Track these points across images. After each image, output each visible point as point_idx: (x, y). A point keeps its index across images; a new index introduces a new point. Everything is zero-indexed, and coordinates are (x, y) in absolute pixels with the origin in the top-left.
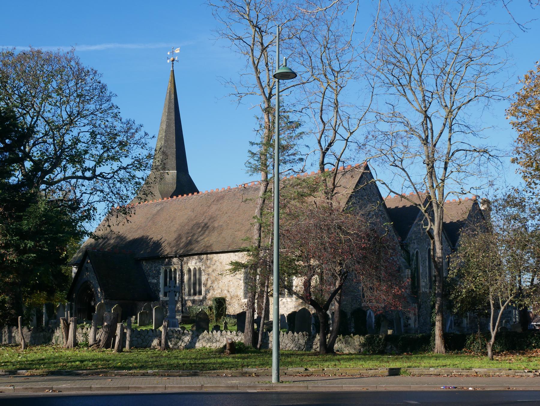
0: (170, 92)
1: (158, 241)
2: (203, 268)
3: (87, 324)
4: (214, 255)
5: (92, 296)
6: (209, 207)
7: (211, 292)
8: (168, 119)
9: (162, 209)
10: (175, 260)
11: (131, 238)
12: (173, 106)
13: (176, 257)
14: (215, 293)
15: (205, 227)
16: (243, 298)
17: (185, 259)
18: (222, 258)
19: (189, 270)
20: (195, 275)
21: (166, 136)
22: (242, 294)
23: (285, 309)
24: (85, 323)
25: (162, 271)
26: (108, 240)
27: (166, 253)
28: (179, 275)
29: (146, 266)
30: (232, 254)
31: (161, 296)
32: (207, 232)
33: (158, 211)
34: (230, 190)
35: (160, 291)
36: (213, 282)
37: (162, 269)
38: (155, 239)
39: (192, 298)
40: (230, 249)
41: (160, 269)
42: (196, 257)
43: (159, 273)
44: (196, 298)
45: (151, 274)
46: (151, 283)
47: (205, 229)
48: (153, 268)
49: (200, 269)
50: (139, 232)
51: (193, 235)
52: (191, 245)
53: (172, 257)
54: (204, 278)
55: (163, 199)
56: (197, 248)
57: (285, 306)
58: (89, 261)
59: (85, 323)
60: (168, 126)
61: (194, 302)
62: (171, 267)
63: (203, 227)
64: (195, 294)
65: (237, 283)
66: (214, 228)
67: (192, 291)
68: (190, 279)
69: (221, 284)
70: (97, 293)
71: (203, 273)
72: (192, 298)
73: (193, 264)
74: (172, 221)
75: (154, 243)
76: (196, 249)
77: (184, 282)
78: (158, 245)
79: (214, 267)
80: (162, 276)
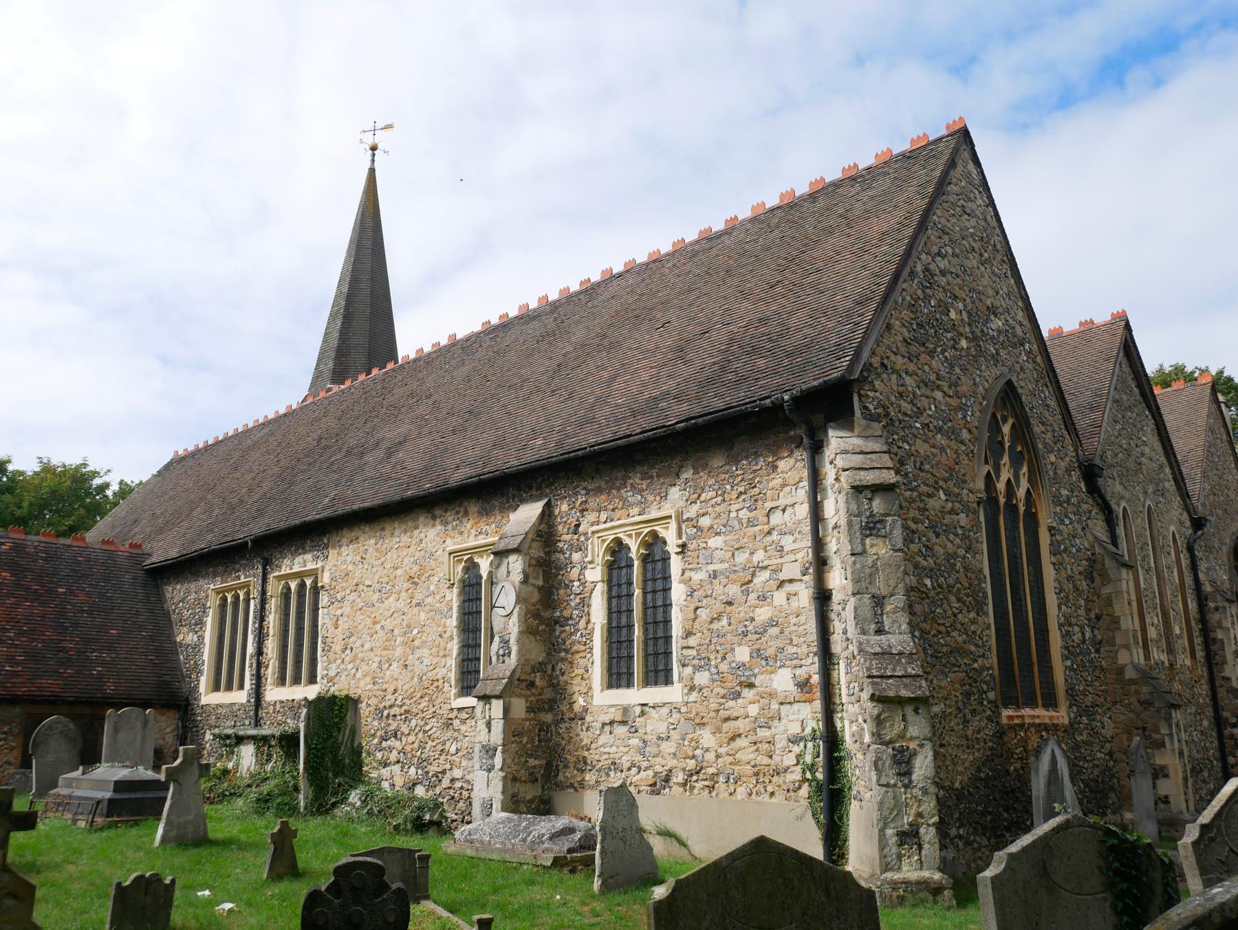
22: (453, 676)
23: (635, 742)
31: (204, 683)
80: (209, 621)
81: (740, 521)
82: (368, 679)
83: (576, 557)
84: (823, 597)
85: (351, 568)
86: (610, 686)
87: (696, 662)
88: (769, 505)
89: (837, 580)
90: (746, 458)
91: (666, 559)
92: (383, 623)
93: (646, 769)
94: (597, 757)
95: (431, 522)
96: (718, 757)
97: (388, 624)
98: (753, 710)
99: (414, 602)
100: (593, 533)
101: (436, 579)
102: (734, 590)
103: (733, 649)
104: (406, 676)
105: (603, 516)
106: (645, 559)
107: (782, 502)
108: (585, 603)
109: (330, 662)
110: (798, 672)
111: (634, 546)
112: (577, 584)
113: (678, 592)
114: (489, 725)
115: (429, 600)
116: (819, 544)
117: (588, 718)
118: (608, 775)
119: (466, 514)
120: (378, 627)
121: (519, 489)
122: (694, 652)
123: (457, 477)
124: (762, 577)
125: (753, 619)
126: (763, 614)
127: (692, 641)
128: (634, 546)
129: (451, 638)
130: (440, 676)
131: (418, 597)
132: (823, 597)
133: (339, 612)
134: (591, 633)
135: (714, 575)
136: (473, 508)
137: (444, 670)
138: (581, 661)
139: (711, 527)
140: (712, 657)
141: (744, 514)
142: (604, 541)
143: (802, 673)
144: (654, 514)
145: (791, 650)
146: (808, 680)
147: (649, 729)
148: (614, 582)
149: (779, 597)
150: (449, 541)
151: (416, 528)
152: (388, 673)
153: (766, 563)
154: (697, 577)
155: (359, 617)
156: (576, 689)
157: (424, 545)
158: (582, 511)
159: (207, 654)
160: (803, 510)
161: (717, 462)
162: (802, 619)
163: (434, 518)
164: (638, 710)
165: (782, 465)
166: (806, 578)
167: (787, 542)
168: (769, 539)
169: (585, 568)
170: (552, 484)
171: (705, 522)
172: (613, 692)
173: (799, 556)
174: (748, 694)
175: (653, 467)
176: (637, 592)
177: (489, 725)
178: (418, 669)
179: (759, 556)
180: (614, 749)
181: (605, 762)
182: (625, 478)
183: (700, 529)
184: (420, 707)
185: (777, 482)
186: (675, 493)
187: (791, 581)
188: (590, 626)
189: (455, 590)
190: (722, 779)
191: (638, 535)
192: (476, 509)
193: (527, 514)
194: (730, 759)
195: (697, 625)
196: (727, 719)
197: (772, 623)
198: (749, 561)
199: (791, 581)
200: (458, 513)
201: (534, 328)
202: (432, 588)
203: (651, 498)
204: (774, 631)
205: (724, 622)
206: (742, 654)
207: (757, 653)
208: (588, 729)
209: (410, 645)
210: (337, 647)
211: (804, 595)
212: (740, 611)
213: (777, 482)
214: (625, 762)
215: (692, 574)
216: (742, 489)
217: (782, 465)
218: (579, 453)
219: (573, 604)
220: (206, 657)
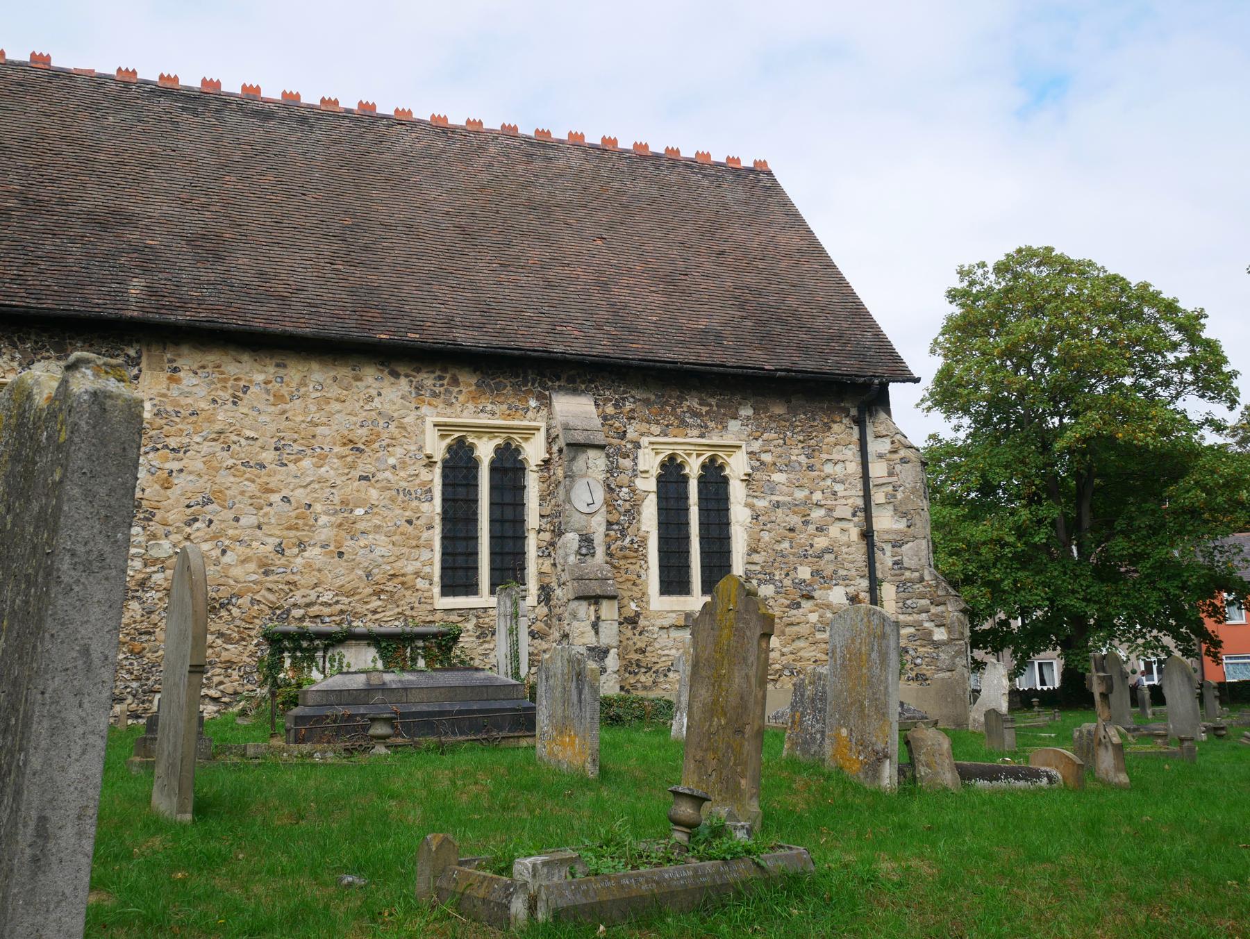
16: (437, 590)
65: (397, 515)
82: (252, 566)
83: (626, 463)
84: (867, 535)
85: (203, 405)
86: (664, 591)
87: (760, 576)
88: (825, 456)
89: (885, 522)
90: (805, 414)
92: (284, 493)
94: (654, 660)
95: (392, 379)
96: (783, 655)
97: (300, 495)
98: (813, 618)
99: (356, 473)
100: (650, 443)
101: (399, 451)
102: (795, 520)
103: (795, 568)
104: (341, 567)
105: (656, 429)
106: (702, 480)
107: (835, 457)
109: (154, 536)
110: (848, 590)
111: (693, 469)
112: (625, 490)
113: (739, 514)
114: (595, 626)
115: (388, 474)
116: (867, 496)
117: (642, 622)
118: (666, 676)
119: (455, 382)
120: (275, 498)
121: (542, 375)
122: (758, 568)
123: (466, 338)
124: (817, 514)
125: (812, 546)
126: (821, 542)
127: (756, 558)
128: (693, 469)
129: (430, 527)
130: (410, 568)
131: (365, 466)
132: (867, 535)
133: (175, 466)
134: (644, 541)
135: (778, 505)
136: (468, 381)
137: (418, 564)
138: (632, 567)
139: (775, 464)
140: (777, 573)
141: (803, 459)
142: (657, 453)
143: (851, 590)
144: (715, 440)
145: (842, 572)
146: (857, 596)
149: (834, 530)
151: (358, 379)
152: (299, 560)
153: (822, 503)
154: (761, 504)
155: (225, 479)
157: (377, 402)
158: (630, 418)
160: (854, 467)
161: (779, 410)
162: (853, 549)
163: (396, 375)
165: (835, 427)
166: (856, 519)
167: (839, 488)
169: (636, 476)
170: (591, 381)
171: (767, 458)
172: (666, 598)
173: (850, 501)
174: (807, 605)
175: (712, 396)
177: (595, 626)
178: (364, 558)
179: (817, 496)
181: (662, 665)
182: (681, 399)
183: (762, 463)
184: (372, 606)
185: (831, 440)
186: (734, 425)
187: (840, 520)
188: (641, 533)
189: (438, 470)
190: (787, 672)
192: (474, 381)
193: (575, 409)
194: (793, 657)
195: (762, 545)
196: (792, 624)
197: (829, 550)
198: (808, 498)
199: (840, 520)
200: (441, 378)
201: (254, 131)
202: (392, 461)
203: (712, 425)
204: (832, 556)
205: (786, 545)
206: (804, 573)
207: (816, 573)
208: (641, 634)
209: (348, 527)
210: (176, 516)
211: (854, 533)
212: (802, 538)
213: (831, 440)
215: (755, 501)
216: (801, 438)
217: (835, 427)
218: (668, 365)
219: (622, 510)
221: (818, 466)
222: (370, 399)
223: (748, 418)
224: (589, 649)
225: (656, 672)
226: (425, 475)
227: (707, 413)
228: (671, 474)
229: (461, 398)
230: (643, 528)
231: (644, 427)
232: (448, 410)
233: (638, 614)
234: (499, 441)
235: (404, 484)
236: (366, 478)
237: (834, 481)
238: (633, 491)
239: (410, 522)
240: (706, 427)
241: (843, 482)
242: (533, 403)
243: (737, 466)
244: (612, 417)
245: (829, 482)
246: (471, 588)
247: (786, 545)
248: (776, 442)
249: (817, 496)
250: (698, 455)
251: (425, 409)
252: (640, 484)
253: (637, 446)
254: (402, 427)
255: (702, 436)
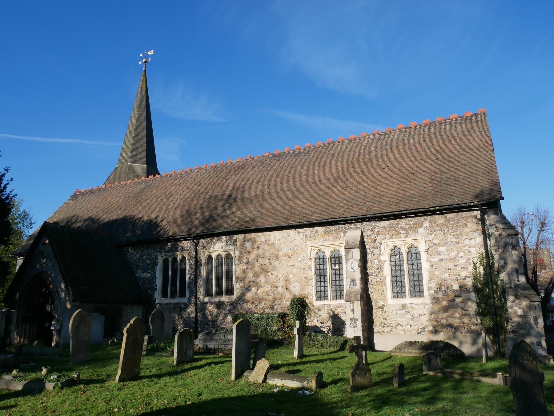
0: (141, 89)
1: (151, 221)
2: (235, 254)
3: (49, 373)
4: (260, 234)
5: (51, 296)
6: (225, 178)
7: (254, 289)
8: (138, 114)
9: (148, 187)
10: (186, 244)
11: (107, 220)
12: (144, 103)
13: (185, 239)
14: (259, 292)
15: (230, 200)
16: (314, 298)
17: (203, 242)
18: (272, 238)
19: (210, 258)
20: (220, 265)
21: (136, 130)
22: (314, 293)
23: (408, 316)
24: (44, 371)
25: (160, 260)
26: (73, 223)
27: (170, 234)
28: (190, 266)
29: (133, 254)
30: (292, 232)
31: (158, 296)
32: (236, 206)
33: (143, 189)
34: (251, 159)
35: (156, 290)
36: (257, 275)
37: (159, 257)
38: (145, 218)
39: (217, 299)
40: (290, 223)
41: (157, 258)
42: (224, 238)
43: (155, 264)
44: (225, 299)
45: (141, 265)
46: (139, 278)
47: (230, 201)
48: (145, 257)
49: (228, 256)
50: (118, 212)
51: (213, 210)
52: (215, 220)
53: (180, 240)
54: (237, 269)
55: (148, 177)
56: (226, 225)
57: (407, 312)
58: (47, 242)
59: (44, 371)
60: (139, 121)
61: (219, 305)
62: (178, 253)
63: (226, 201)
64: (220, 293)
66: (247, 201)
67: (214, 289)
68: (209, 273)
69: (272, 278)
70: (58, 292)
71: (236, 262)
72: (217, 299)
73: (218, 248)
74: (168, 198)
75: (146, 223)
76: (225, 226)
77: (200, 275)
78: (152, 225)
79: (260, 251)
81: (452, 242)
91: (418, 253)
93: (414, 326)
101: (301, 256)
102: (451, 265)
105: (388, 237)
108: (380, 268)
112: (377, 261)
113: (425, 266)
114: (353, 311)
117: (385, 309)
125: (459, 275)
134: (385, 278)
141: (454, 240)
147: (415, 312)
148: (392, 260)
150: (308, 242)
156: (379, 298)
159: (159, 283)
164: (409, 306)
168: (464, 248)
171: (436, 241)
176: (406, 265)
180: (398, 319)
181: (394, 324)
189: (313, 261)
191: (405, 245)
195: (435, 276)
198: (456, 255)
202: (299, 260)
214: (404, 322)
217: (469, 224)
220: (157, 283)
221: (461, 242)
222: (292, 241)
223: (427, 227)
224: (351, 319)
225: (392, 326)
226: (309, 263)
227: (409, 228)
228: (395, 252)
229: (319, 237)
230: (385, 274)
231: (383, 237)
232: (314, 242)
233: (384, 305)
234: (332, 249)
235: (303, 266)
236: (293, 266)
237: (470, 247)
238: (380, 261)
239: (306, 278)
240: (408, 233)
241: (474, 247)
242: (342, 235)
243: (422, 247)
244: (370, 235)
245: (467, 248)
246: (325, 298)
247: (447, 275)
248: (440, 235)
249: (461, 254)
250: (405, 245)
251: (308, 242)
252: (382, 258)
253: (381, 244)
254: (301, 248)
255: (407, 237)
